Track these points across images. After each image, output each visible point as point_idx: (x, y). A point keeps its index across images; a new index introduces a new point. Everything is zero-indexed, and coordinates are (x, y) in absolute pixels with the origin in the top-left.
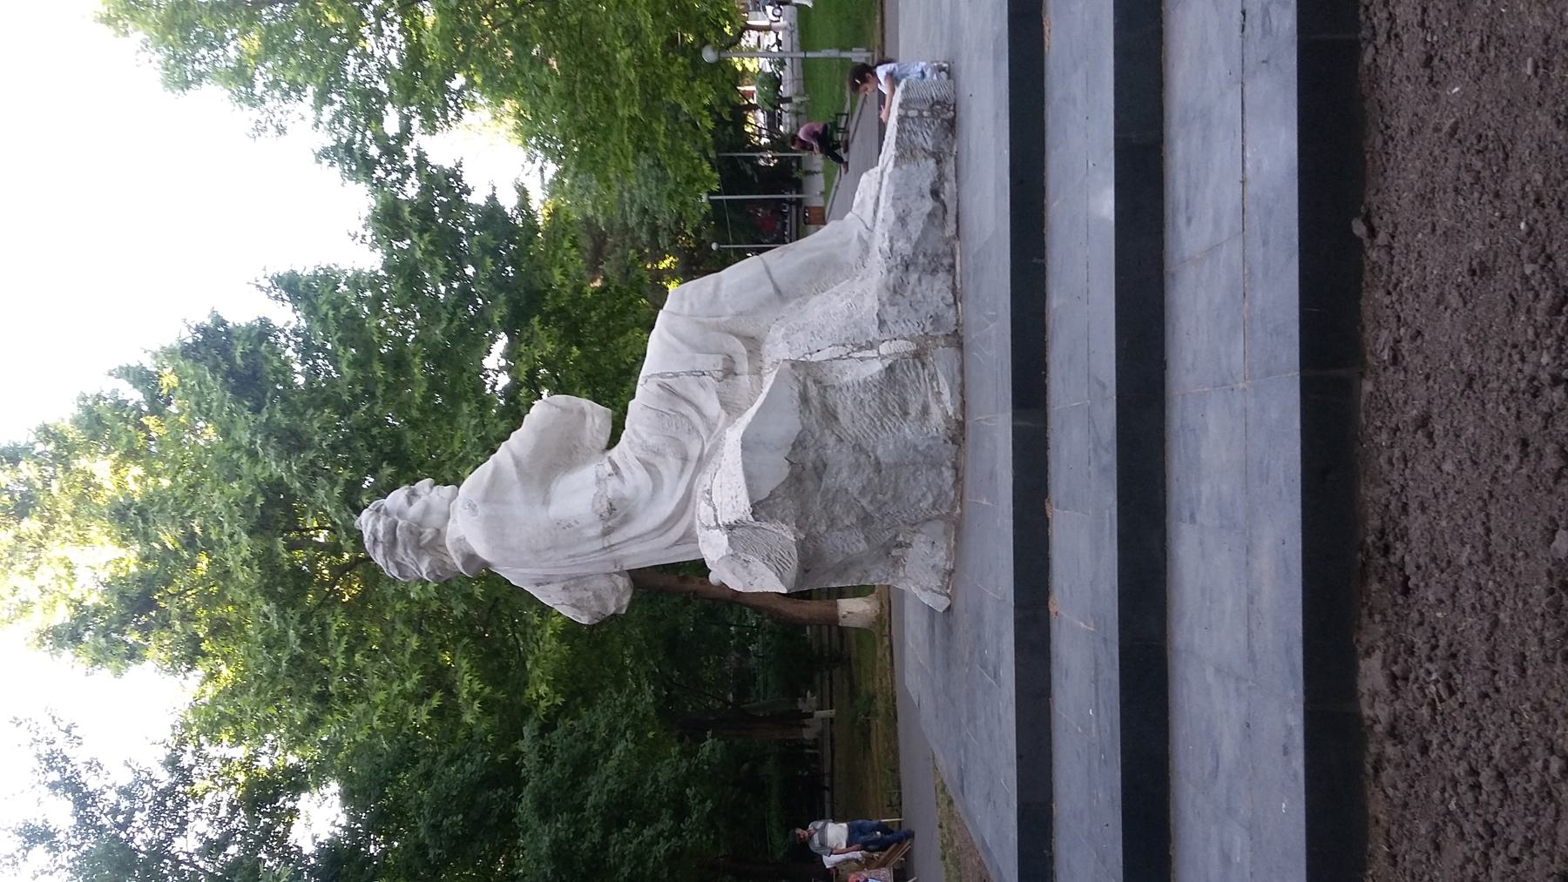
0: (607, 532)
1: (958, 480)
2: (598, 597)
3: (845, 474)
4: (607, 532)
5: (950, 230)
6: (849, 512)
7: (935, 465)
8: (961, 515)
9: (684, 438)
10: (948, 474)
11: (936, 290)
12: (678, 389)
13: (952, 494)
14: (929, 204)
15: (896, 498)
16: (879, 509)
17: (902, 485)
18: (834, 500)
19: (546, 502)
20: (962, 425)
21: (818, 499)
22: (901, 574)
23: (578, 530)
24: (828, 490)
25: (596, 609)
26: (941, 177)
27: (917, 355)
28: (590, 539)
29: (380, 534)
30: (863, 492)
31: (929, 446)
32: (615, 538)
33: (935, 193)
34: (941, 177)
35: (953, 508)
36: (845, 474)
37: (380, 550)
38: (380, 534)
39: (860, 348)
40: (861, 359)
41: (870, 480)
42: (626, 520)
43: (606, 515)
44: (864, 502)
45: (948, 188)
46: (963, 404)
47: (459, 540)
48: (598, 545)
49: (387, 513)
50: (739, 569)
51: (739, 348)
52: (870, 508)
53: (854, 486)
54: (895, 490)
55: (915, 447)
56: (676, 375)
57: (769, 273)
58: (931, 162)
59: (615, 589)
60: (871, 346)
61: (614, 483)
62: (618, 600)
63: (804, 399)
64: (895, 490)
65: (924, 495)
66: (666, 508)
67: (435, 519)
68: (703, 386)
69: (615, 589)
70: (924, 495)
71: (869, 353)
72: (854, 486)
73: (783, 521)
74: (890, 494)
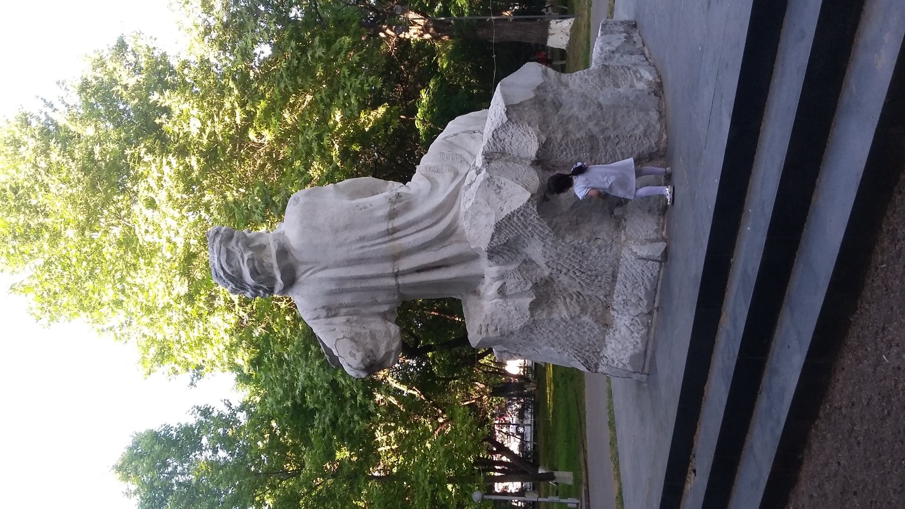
0: (392, 215)
1: (662, 115)
2: (373, 336)
3: (575, 109)
4: (392, 215)
6: (579, 130)
7: (644, 110)
8: (667, 141)
9: (458, 166)
10: (654, 115)
12: (456, 142)
13: (658, 126)
15: (616, 126)
16: (603, 131)
17: (619, 119)
18: (568, 122)
20: (660, 85)
21: (556, 118)
22: (623, 238)
23: (372, 211)
24: (563, 116)
25: (370, 346)
28: (379, 220)
29: (222, 231)
30: (589, 118)
31: (637, 96)
32: (398, 222)
35: (660, 137)
36: (575, 109)
37: (218, 239)
38: (222, 231)
41: (595, 113)
42: (408, 207)
43: (394, 199)
44: (591, 125)
47: (279, 234)
48: (384, 226)
50: (493, 196)
52: (595, 130)
53: (583, 115)
54: (615, 121)
55: (627, 98)
56: (456, 135)
59: (388, 333)
62: (389, 344)
64: (615, 121)
65: (637, 126)
66: (440, 197)
68: (473, 138)
69: (388, 333)
70: (637, 126)
72: (583, 115)
73: (529, 124)
74: (610, 122)
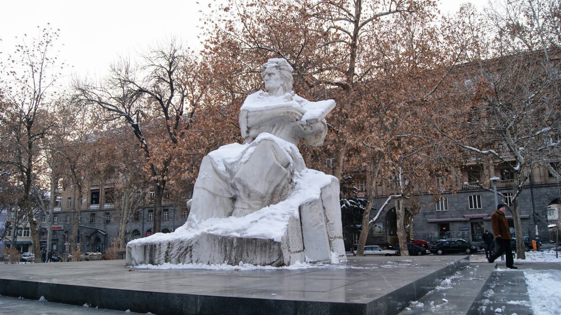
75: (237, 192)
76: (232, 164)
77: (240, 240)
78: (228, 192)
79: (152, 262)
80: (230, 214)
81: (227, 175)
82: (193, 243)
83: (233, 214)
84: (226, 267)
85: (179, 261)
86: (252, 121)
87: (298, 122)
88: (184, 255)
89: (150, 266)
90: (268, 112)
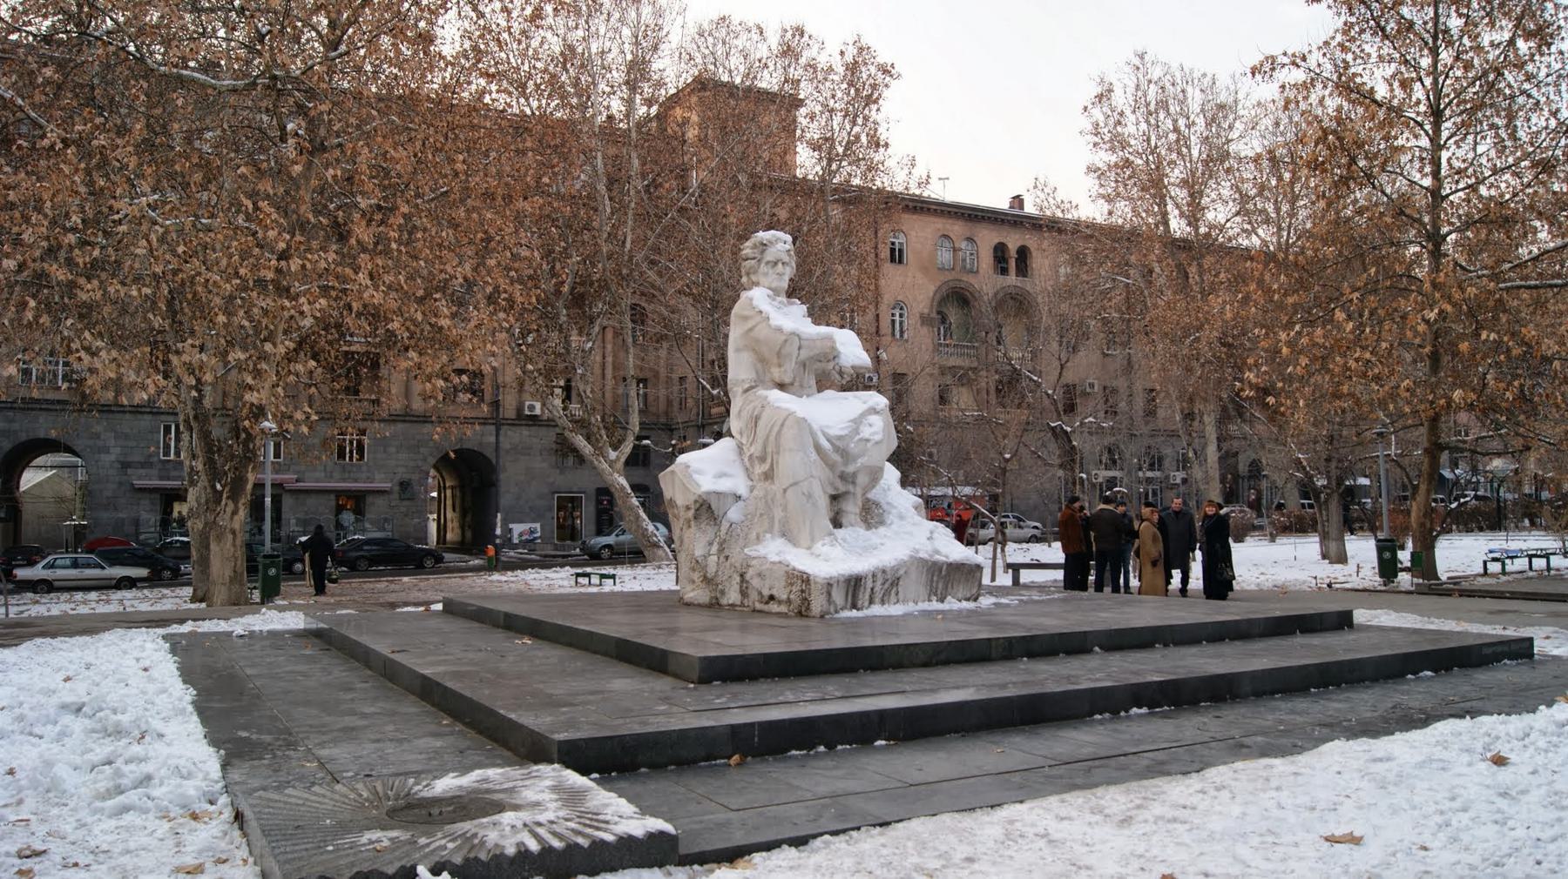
5: (758, 606)
11: (733, 596)
14: (766, 593)
19: (738, 350)
26: (780, 602)
27: (705, 577)
33: (772, 598)
34: (780, 602)
39: (721, 544)
40: (711, 544)
45: (774, 607)
46: (688, 605)
49: (763, 252)
51: (766, 467)
57: (795, 484)
58: (784, 597)
60: (721, 550)
61: (740, 390)
63: (688, 508)
67: (762, 280)
71: (715, 548)
75: (851, 488)
76: (840, 438)
77: (950, 565)
78: (832, 484)
79: (854, 606)
80: (837, 524)
81: (836, 457)
82: (901, 572)
83: (844, 521)
84: (935, 605)
85: (883, 602)
86: (804, 354)
87: (831, 365)
88: (887, 593)
89: (854, 613)
90: (818, 344)
